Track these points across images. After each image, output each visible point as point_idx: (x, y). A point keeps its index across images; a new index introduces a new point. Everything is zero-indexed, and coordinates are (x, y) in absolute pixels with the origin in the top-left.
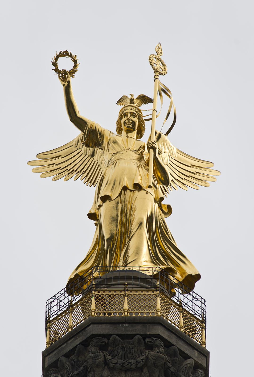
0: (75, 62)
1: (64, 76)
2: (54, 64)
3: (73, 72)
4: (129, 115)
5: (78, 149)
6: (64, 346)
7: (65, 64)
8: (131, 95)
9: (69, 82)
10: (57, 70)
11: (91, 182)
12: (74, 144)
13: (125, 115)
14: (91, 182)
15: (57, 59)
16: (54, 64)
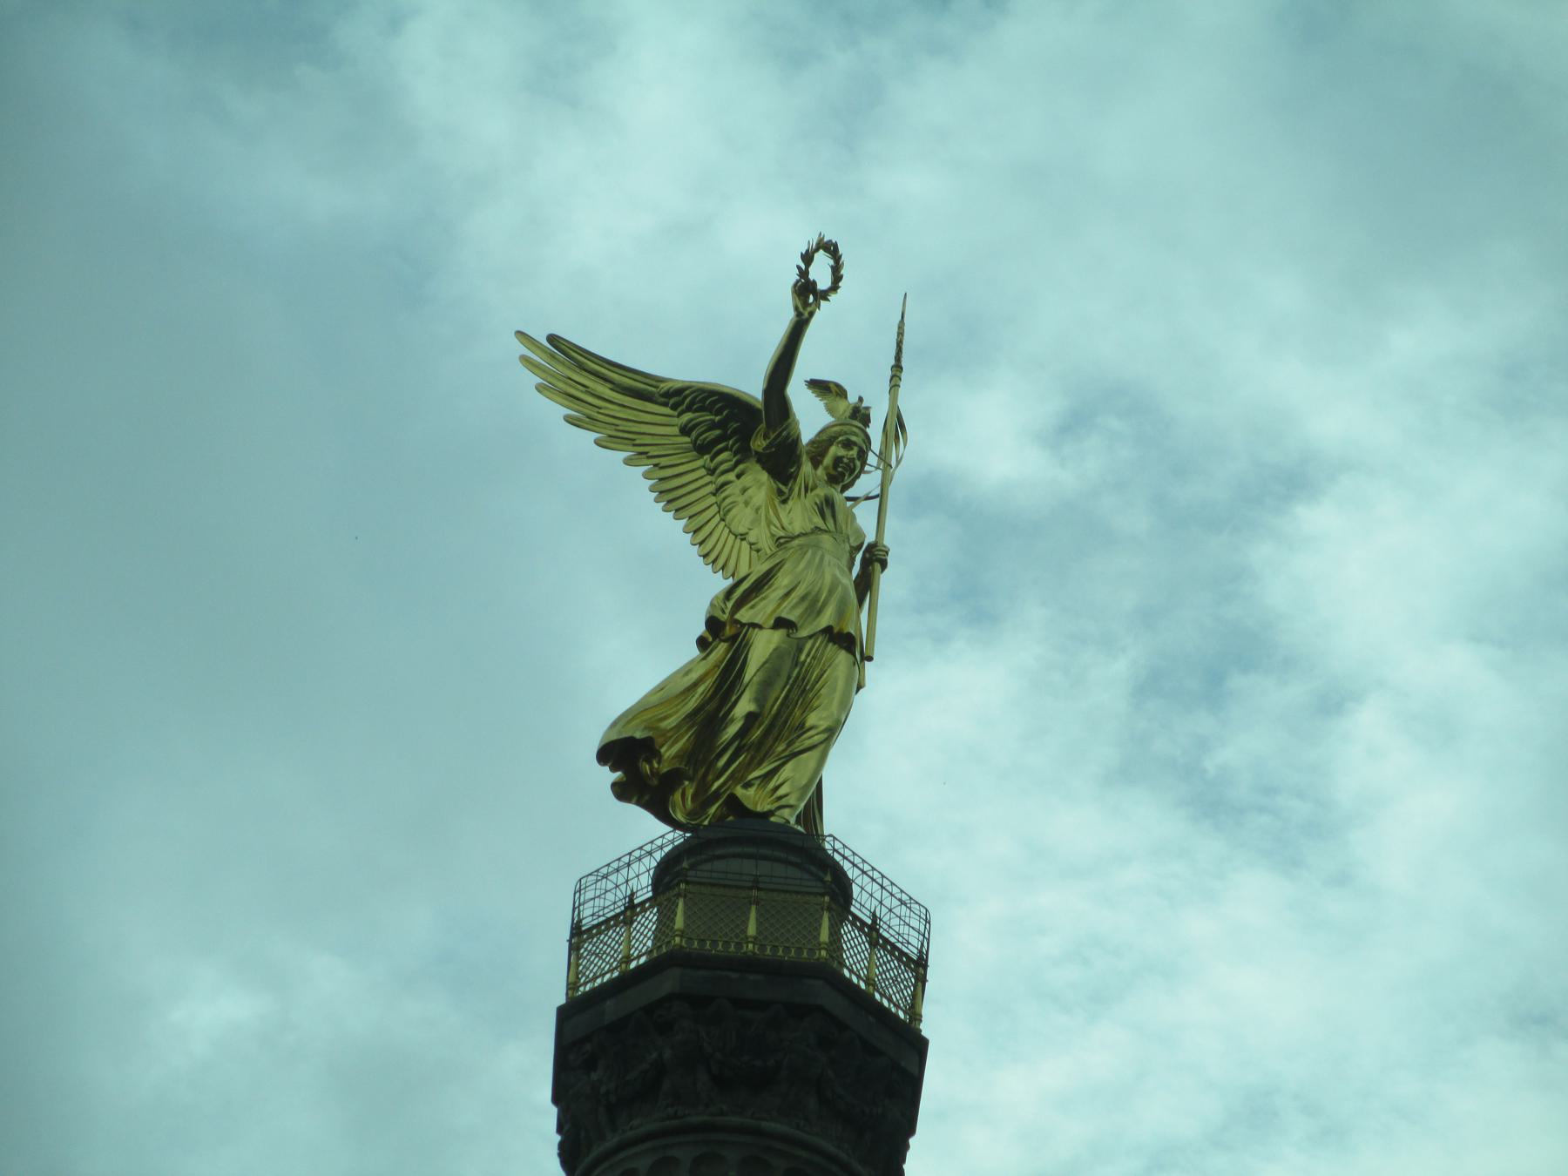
0: (837, 277)
1: (806, 291)
2: (808, 258)
3: (824, 295)
4: (856, 449)
5: (665, 405)
6: (734, 975)
7: (821, 273)
8: (861, 399)
9: (811, 314)
10: (803, 274)
11: (669, 502)
12: (664, 387)
13: (848, 445)
14: (669, 502)
15: (817, 250)
16: (808, 258)
